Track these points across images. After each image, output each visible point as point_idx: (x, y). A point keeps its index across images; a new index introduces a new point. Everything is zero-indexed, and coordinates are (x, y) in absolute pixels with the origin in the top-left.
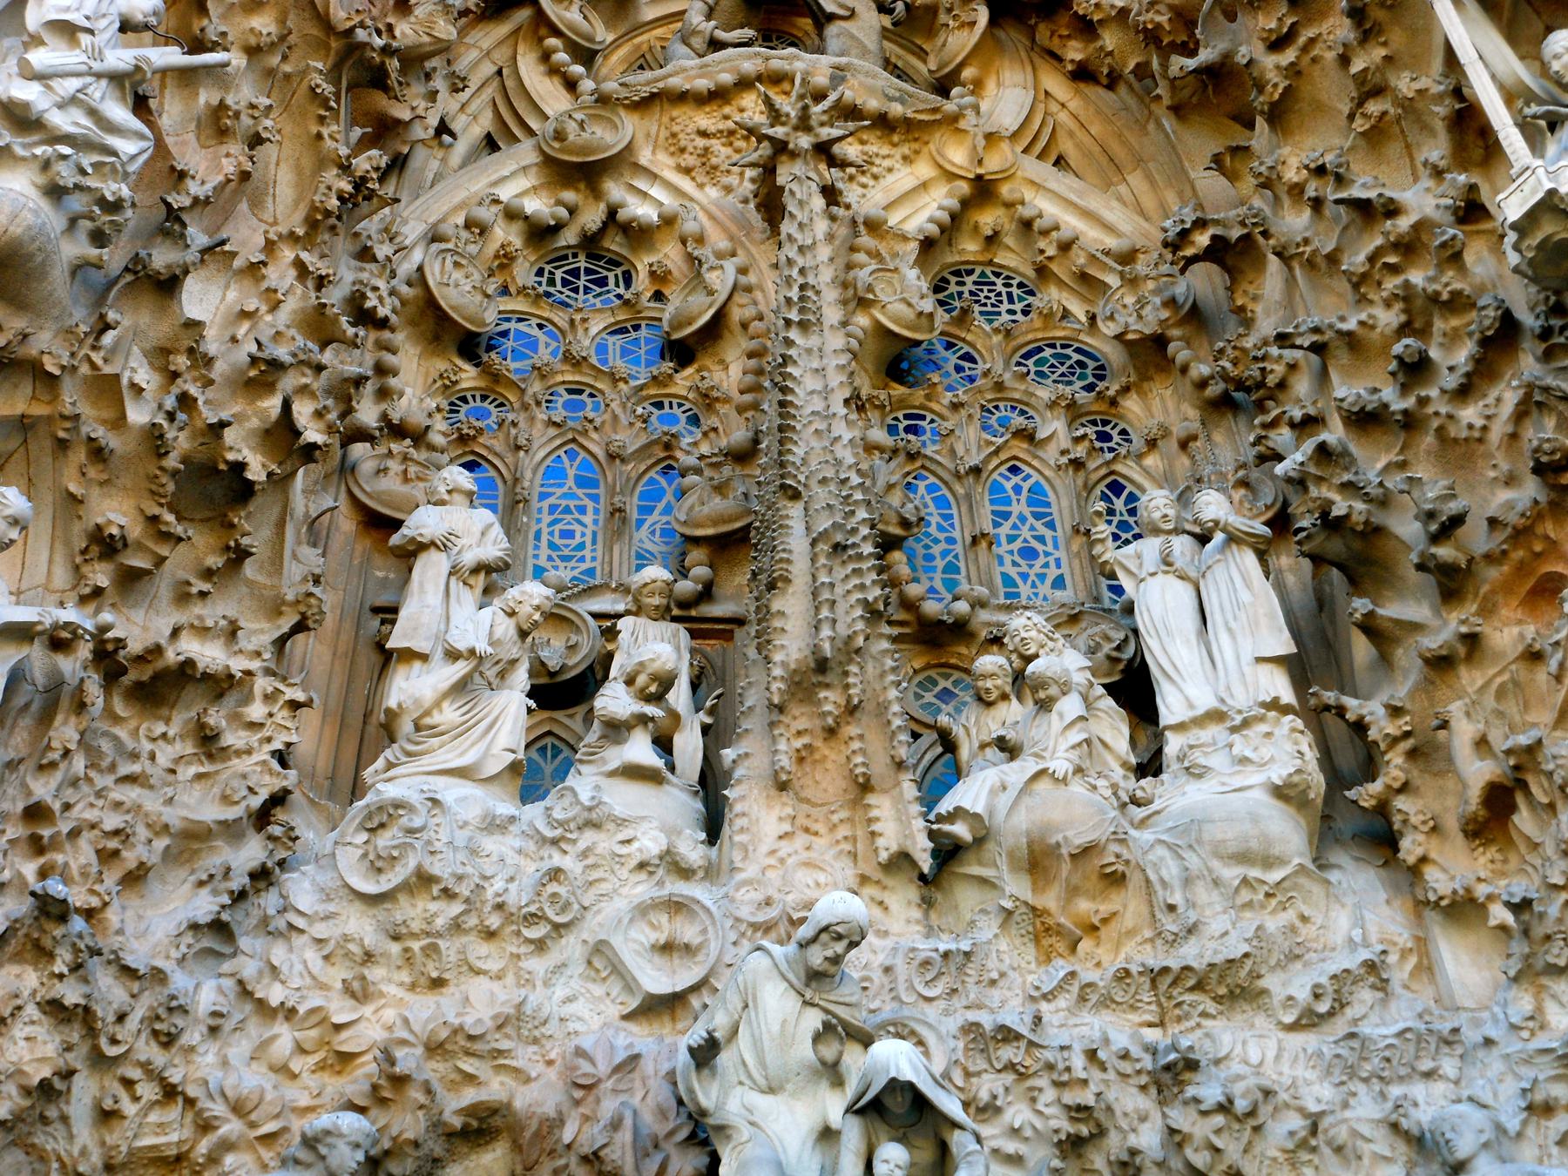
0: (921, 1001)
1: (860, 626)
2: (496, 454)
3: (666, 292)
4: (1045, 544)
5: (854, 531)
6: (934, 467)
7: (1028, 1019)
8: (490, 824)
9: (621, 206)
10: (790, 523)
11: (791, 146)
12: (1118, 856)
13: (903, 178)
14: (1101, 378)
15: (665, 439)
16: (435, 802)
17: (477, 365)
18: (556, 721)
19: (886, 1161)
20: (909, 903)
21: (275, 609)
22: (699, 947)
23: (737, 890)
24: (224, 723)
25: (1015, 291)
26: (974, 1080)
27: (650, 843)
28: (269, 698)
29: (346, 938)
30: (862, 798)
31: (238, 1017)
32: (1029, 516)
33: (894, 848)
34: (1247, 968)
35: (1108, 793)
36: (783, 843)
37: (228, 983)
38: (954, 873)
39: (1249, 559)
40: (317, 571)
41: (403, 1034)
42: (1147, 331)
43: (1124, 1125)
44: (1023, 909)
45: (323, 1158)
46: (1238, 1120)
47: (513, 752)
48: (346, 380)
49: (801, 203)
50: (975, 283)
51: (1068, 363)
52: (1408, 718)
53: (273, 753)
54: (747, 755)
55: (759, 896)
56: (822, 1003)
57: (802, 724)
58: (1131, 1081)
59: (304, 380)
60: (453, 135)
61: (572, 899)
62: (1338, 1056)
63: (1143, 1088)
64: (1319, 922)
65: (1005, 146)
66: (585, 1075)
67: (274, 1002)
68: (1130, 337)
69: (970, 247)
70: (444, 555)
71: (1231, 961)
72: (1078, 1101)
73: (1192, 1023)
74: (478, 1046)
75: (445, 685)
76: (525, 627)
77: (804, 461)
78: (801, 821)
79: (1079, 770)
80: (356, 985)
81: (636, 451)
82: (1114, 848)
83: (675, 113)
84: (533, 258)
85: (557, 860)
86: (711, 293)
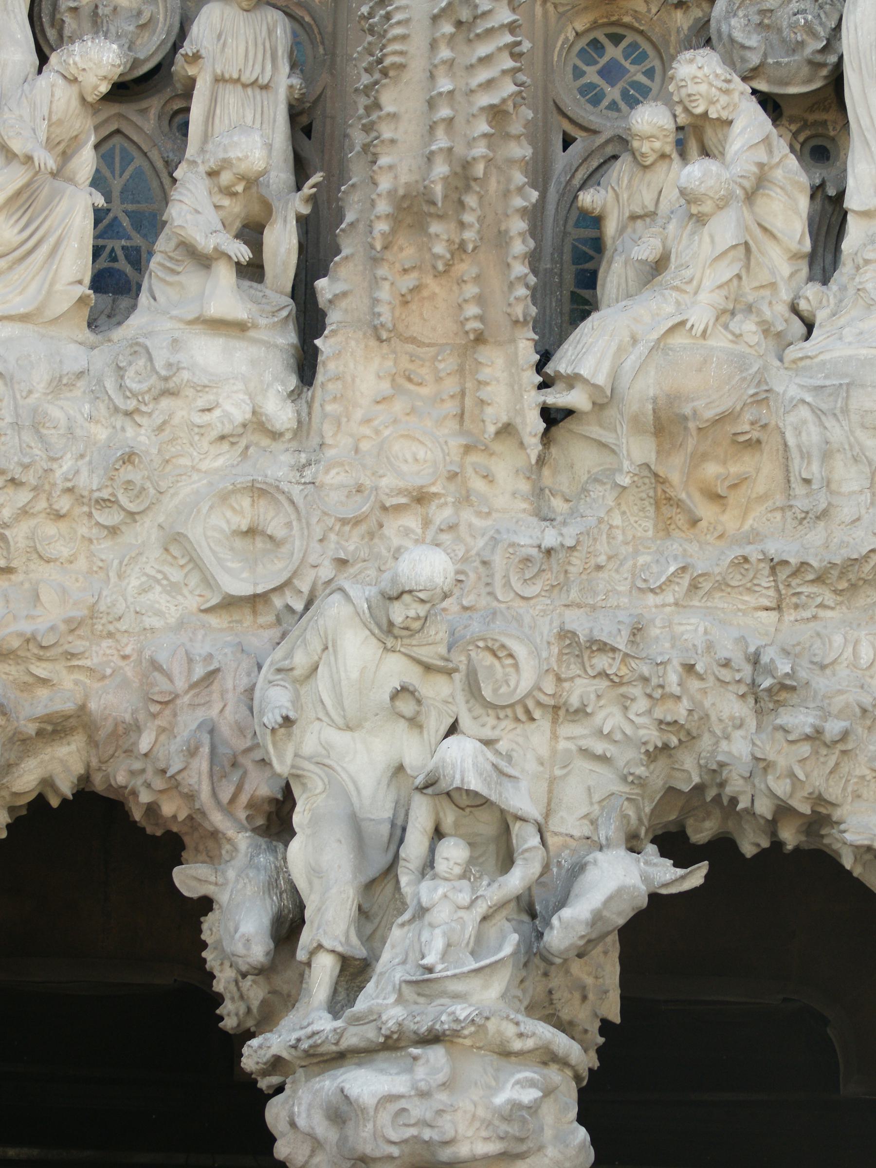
0: (518, 600)
7: (625, 633)
8: (57, 386)
18: (127, 119)
19: (447, 859)
23: (327, 472)
26: (566, 685)
36: (380, 407)
38: (570, 431)
44: (646, 473)
46: (826, 745)
47: (80, 282)
54: (344, 294)
56: (402, 650)
58: (730, 688)
61: (148, 484)
71: (856, 560)
72: (669, 719)
73: (807, 614)
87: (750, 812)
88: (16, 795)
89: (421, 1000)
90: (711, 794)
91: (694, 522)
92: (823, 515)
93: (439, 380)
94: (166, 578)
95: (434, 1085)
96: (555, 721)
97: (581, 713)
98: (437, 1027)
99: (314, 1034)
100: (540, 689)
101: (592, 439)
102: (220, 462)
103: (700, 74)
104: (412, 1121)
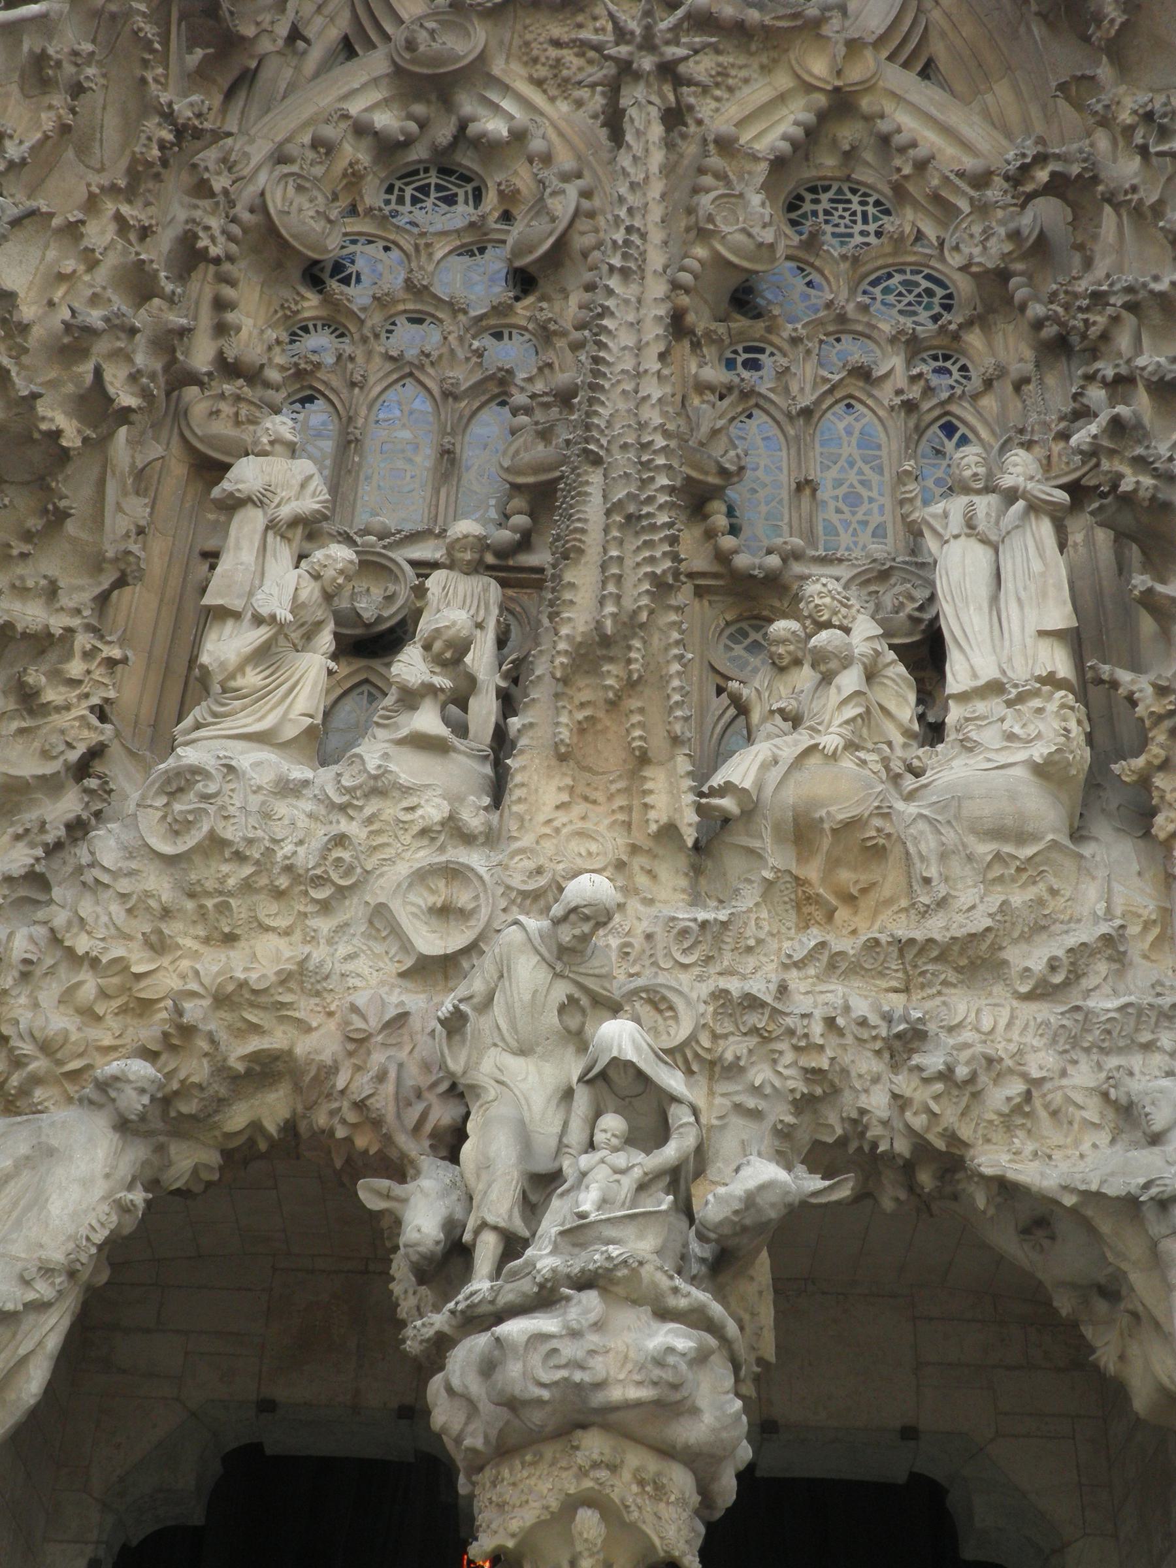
1: (645, 601)
2: (332, 389)
3: (515, 212)
4: (871, 489)
5: (650, 500)
6: (767, 406)
7: (773, 987)
9: (473, 119)
10: (588, 489)
11: (635, 66)
12: (879, 830)
13: (758, 92)
14: (948, 308)
15: (499, 375)
16: (230, 769)
17: (320, 292)
19: (605, 1131)
20: (677, 871)
21: (97, 564)
22: (474, 911)
23: (512, 858)
24: (43, 679)
25: (871, 210)
26: (721, 1042)
27: (433, 810)
28: (88, 655)
29: (148, 894)
30: (640, 770)
31: (49, 962)
32: (858, 458)
33: (664, 819)
34: (988, 942)
35: (878, 767)
36: (559, 813)
37: (41, 932)
39: (1045, 528)
40: (142, 523)
41: (194, 986)
42: (990, 265)
43: (858, 1085)
45: (113, 1100)
46: (957, 1085)
47: (311, 716)
48: (170, 331)
49: (638, 133)
50: (832, 201)
51: (917, 291)
52: (1172, 698)
53: (92, 709)
54: (531, 725)
55: (530, 865)
57: (585, 696)
59: (120, 344)
60: (307, 41)
62: (1063, 1026)
63: (878, 1053)
64: (1068, 894)
65: (868, 54)
66: (357, 1030)
67: (80, 951)
68: (974, 269)
69: (828, 163)
70: (259, 513)
71: (973, 935)
73: (934, 991)
74: (263, 999)
75: (248, 650)
76: (329, 590)
77: (609, 424)
78: (581, 789)
79: (851, 746)
80: (154, 938)
81: (471, 388)
82: (877, 822)
83: (528, 21)
84: (383, 175)
85: (343, 826)
86: (553, 219)
87: (890, 1156)
88: (229, 1136)
89: (576, 1250)
90: (853, 1146)
91: (830, 916)
92: (942, 903)
93: (611, 798)
94: (370, 949)
95: (585, 1324)
96: (711, 1078)
97: (734, 1070)
98: (591, 1267)
99: (472, 1294)
100: (698, 1042)
101: (743, 847)
102: (422, 853)
103: (824, 590)
104: (563, 1361)
